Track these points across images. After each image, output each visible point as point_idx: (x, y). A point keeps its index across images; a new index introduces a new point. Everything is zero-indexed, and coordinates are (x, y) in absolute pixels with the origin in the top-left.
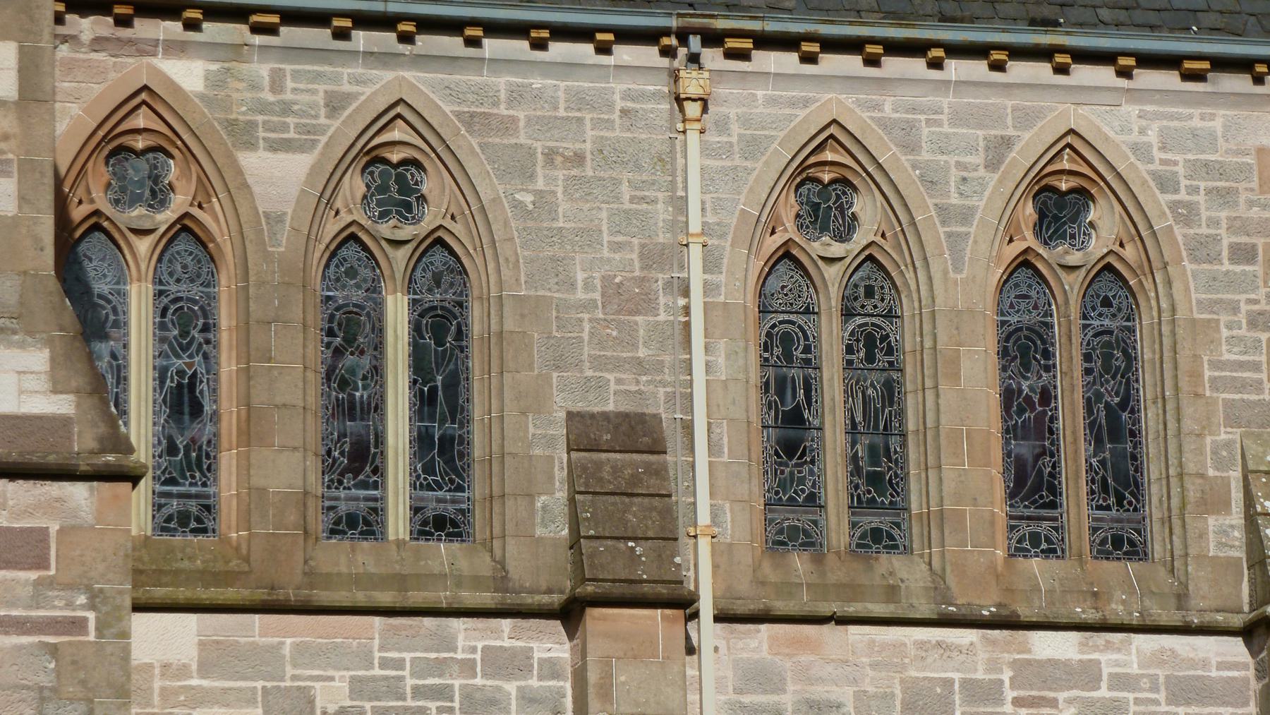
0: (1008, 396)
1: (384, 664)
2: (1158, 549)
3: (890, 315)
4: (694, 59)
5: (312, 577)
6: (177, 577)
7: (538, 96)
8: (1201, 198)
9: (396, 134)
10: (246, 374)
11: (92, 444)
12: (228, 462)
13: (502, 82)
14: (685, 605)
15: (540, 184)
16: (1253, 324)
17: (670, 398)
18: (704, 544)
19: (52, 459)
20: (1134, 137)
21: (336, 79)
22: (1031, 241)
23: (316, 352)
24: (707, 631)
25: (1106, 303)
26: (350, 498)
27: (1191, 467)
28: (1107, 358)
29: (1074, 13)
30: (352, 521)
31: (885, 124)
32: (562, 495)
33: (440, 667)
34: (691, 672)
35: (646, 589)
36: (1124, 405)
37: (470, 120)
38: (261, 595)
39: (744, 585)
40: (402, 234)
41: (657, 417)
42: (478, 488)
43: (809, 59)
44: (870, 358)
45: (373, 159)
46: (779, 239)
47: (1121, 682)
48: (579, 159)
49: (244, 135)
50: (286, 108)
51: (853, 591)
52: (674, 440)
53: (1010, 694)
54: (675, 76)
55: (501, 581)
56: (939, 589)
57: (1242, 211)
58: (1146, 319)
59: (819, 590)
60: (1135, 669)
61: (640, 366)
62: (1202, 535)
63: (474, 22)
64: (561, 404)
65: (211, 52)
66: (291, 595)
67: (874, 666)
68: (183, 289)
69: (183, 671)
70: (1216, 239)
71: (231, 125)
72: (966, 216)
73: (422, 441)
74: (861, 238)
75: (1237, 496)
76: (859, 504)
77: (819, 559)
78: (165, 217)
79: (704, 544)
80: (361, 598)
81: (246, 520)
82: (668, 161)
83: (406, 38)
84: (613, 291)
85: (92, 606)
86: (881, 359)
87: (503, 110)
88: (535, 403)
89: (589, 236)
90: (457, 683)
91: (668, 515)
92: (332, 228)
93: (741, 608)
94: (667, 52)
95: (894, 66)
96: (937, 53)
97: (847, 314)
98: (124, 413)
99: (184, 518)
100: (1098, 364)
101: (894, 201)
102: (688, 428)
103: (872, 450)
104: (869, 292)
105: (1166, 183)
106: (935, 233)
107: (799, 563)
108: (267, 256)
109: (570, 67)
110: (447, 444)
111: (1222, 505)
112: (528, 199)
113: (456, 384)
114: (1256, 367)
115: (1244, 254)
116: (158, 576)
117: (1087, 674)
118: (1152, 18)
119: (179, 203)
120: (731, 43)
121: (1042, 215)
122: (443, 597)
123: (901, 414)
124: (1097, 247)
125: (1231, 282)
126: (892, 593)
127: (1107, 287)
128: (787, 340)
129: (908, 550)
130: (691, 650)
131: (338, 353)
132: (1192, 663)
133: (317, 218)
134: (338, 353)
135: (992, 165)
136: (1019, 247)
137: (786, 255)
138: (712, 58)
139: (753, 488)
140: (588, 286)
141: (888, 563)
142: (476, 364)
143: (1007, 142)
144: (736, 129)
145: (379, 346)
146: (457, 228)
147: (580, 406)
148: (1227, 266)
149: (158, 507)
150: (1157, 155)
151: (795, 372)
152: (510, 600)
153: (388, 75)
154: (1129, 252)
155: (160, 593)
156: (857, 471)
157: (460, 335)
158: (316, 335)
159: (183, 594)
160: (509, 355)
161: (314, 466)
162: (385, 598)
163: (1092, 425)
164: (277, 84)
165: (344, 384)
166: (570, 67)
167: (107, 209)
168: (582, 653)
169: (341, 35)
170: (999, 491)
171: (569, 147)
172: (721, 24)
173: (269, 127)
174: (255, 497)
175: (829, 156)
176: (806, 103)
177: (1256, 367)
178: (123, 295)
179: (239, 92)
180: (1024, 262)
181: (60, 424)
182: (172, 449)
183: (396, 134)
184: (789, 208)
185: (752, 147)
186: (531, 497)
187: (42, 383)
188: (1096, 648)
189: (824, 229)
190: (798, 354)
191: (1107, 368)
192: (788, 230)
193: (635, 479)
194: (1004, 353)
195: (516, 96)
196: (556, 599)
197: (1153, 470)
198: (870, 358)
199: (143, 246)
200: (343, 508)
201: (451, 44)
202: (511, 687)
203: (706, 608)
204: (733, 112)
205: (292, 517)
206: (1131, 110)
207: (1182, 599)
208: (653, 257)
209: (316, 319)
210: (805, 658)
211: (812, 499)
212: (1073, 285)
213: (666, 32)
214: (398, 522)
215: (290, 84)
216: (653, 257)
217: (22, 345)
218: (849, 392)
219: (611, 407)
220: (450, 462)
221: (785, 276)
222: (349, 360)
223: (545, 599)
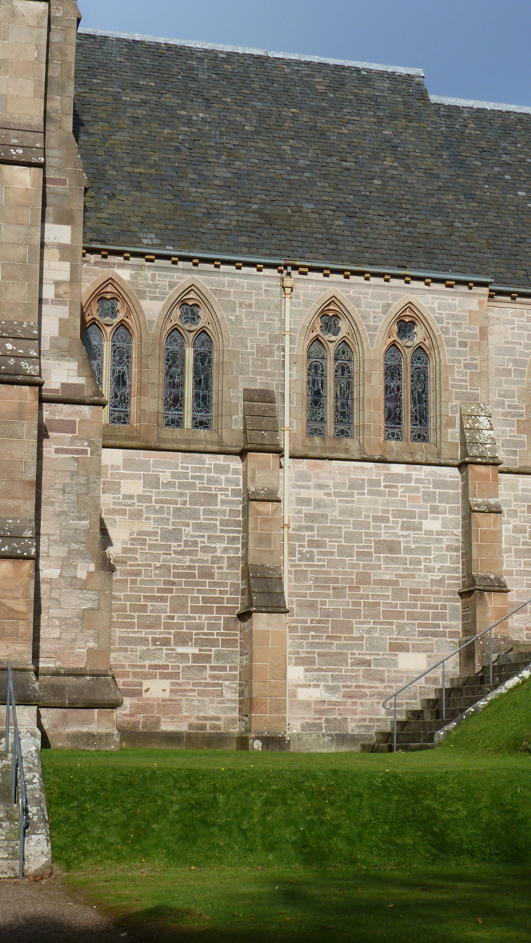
0: (387, 388)
1: (182, 468)
2: (432, 439)
3: (350, 360)
4: (289, 274)
5: (160, 439)
6: (117, 437)
7: (238, 284)
8: (450, 326)
9: (191, 296)
10: (140, 372)
11: (90, 393)
12: (134, 400)
13: (226, 280)
14: (280, 452)
15: (237, 313)
16: (465, 367)
17: (277, 385)
18: (287, 433)
19: (77, 398)
20: (430, 305)
21: (172, 277)
22: (395, 337)
23: (163, 366)
24: (287, 461)
25: (419, 359)
26: (173, 414)
27: (443, 413)
28: (419, 376)
29: (412, 264)
30: (173, 421)
31: (350, 298)
32: (241, 415)
33: (200, 470)
34: (281, 474)
35: (267, 447)
36: (423, 392)
37: (215, 292)
38: (143, 444)
39: (299, 447)
40: (192, 329)
41: (273, 391)
42: (214, 412)
43: (326, 275)
44: (343, 374)
45: (183, 303)
46: (315, 334)
47: (418, 481)
48: (250, 305)
49: (142, 294)
50: (156, 286)
51: (334, 449)
52: (278, 398)
53: (383, 484)
54: (282, 279)
55: (220, 442)
56: (362, 450)
57: (463, 330)
58: (431, 365)
59: (323, 449)
60: (423, 477)
61: (268, 374)
62: (446, 435)
63: (218, 260)
64: (242, 386)
65: (133, 266)
66: (153, 444)
67: (340, 474)
68: (121, 344)
69: (118, 468)
70: (455, 339)
71: (138, 291)
72: (375, 328)
73: (196, 396)
74: (341, 335)
75: (458, 422)
76: (338, 422)
77: (324, 439)
78: (116, 321)
79: (287, 433)
80: (175, 446)
81: (139, 420)
82: (279, 307)
83: (195, 264)
84: (260, 349)
85: (89, 446)
86: (346, 375)
87: (226, 289)
88: (233, 385)
89: (253, 331)
90: (205, 475)
91: (275, 423)
92: (169, 326)
93: (298, 454)
94: (280, 272)
95: (354, 279)
96: (368, 275)
97: (336, 359)
98: (101, 384)
99: (119, 419)
100: (416, 378)
101: (352, 323)
102: (283, 395)
103: (343, 405)
104: (343, 352)
105: (439, 320)
106: (365, 334)
107: (317, 440)
108: (148, 334)
109: (249, 275)
110: (204, 397)
111: (453, 425)
112: (233, 318)
113: (208, 378)
114: (466, 381)
115: (463, 344)
116: (111, 437)
117: (408, 478)
118: (437, 266)
119: (121, 316)
120: (301, 269)
121: (400, 329)
122: (202, 447)
123: (352, 393)
124: (417, 340)
125: (459, 353)
126: (347, 451)
127: (419, 354)
128: (316, 367)
129: (352, 437)
130: (281, 467)
131: (170, 366)
132: (441, 476)
133: (164, 323)
134: (170, 366)
135: (384, 312)
136: (392, 339)
137: (317, 339)
138: (295, 274)
139: (303, 416)
140: (252, 347)
141: (346, 441)
142: (214, 372)
143: (389, 305)
144: (302, 297)
145: (183, 365)
146: (210, 327)
147: (248, 387)
148: (458, 348)
149: (111, 415)
150: (437, 311)
151: (319, 378)
152: (224, 449)
153: (189, 276)
154: (427, 342)
155: (111, 442)
156: (337, 411)
157: (210, 362)
158: (163, 361)
159: (118, 443)
160: (225, 369)
161: (161, 403)
162: (183, 447)
163: (413, 398)
164: (153, 278)
165: (171, 377)
166: (249, 275)
167: (98, 317)
168: (246, 467)
169: (174, 263)
170: (383, 419)
171: (247, 301)
172: (298, 263)
173: (150, 292)
174: (142, 412)
175: (332, 307)
176: (325, 290)
177: (466, 381)
178: (102, 345)
179: (141, 280)
180: (393, 345)
181: (81, 386)
182: (116, 396)
183: (191, 296)
184: (318, 324)
185: (307, 304)
186: (231, 416)
187: (75, 373)
188: (411, 470)
189: (329, 331)
190: (319, 372)
191: (418, 379)
192: (318, 331)
193: (265, 411)
194: (386, 374)
195: (230, 284)
196: (238, 449)
197: (432, 413)
198: (343, 374)
199: (109, 330)
200: (170, 417)
201: (210, 267)
202: (223, 477)
203: (287, 454)
204: (301, 292)
205: (154, 419)
206: (429, 296)
207: (439, 455)
208: (274, 339)
209: (164, 355)
210: (318, 471)
211: (322, 419)
212: (409, 352)
213: (280, 265)
214: (188, 422)
215: (157, 278)
216: (274, 339)
217: (69, 361)
218: (336, 385)
219: (258, 387)
220: (205, 403)
221: (316, 346)
222: (174, 369)
223: (234, 449)
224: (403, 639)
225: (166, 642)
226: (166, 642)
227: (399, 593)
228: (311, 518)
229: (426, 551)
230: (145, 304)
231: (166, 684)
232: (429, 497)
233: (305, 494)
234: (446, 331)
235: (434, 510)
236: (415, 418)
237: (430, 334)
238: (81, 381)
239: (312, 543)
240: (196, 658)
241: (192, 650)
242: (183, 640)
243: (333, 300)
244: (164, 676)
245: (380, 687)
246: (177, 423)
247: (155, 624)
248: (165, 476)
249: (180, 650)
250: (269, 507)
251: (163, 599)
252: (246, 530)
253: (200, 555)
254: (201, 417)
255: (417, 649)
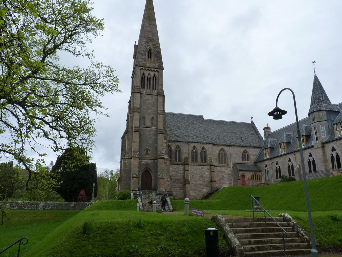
101: (196, 149)
117: (204, 167)
224: (203, 187)
225: (175, 188)
226: (175, 188)
227: (203, 182)
228: (192, 172)
229: (206, 176)
230: (172, 147)
231: (176, 193)
232: (206, 170)
233: (191, 170)
234: (208, 149)
235: (207, 171)
236: (204, 160)
237: (206, 150)
238: (168, 157)
239: (193, 176)
240: (179, 190)
241: (179, 189)
242: (177, 188)
243: (194, 146)
244: (176, 192)
245: (201, 193)
246: (176, 161)
247: (174, 185)
248: (175, 168)
249: (177, 189)
250: (188, 171)
251: (175, 183)
252: (185, 174)
253: (179, 177)
254: (179, 160)
255: (205, 188)
